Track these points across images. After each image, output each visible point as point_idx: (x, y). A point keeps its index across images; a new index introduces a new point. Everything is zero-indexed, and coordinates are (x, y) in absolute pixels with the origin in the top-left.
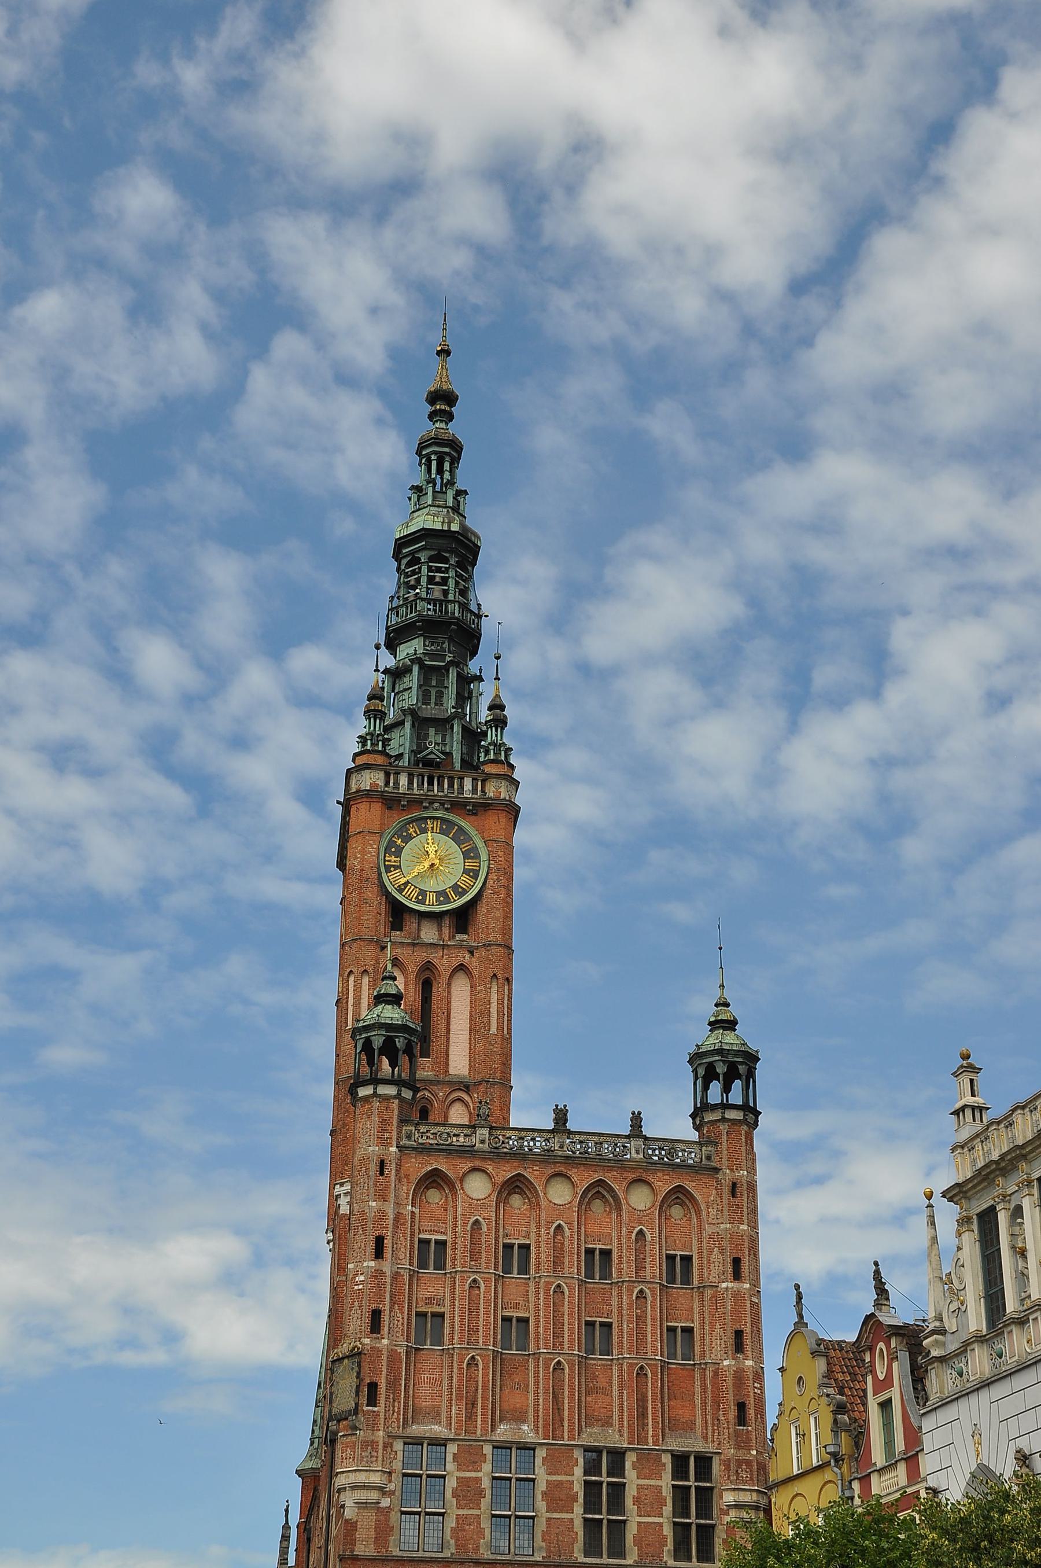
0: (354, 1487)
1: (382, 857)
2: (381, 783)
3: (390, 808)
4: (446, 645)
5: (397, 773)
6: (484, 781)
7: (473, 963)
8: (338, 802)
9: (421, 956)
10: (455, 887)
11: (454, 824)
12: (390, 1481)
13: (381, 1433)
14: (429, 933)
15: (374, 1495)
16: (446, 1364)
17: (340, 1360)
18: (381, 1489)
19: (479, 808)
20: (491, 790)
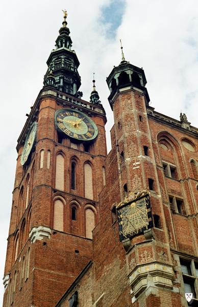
0: (155, 273)
1: (55, 117)
2: (56, 95)
3: (58, 105)
4: (71, 80)
5: (62, 96)
6: (94, 108)
7: (94, 161)
8: (27, 115)
9: (73, 153)
10: (85, 135)
11: (84, 117)
12: (176, 278)
13: (168, 245)
14: (74, 146)
15: (168, 282)
16: (192, 224)
17: (126, 205)
18: (173, 280)
19: (93, 115)
20: (97, 110)
